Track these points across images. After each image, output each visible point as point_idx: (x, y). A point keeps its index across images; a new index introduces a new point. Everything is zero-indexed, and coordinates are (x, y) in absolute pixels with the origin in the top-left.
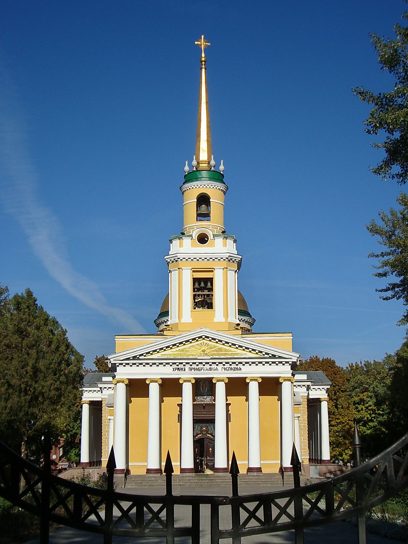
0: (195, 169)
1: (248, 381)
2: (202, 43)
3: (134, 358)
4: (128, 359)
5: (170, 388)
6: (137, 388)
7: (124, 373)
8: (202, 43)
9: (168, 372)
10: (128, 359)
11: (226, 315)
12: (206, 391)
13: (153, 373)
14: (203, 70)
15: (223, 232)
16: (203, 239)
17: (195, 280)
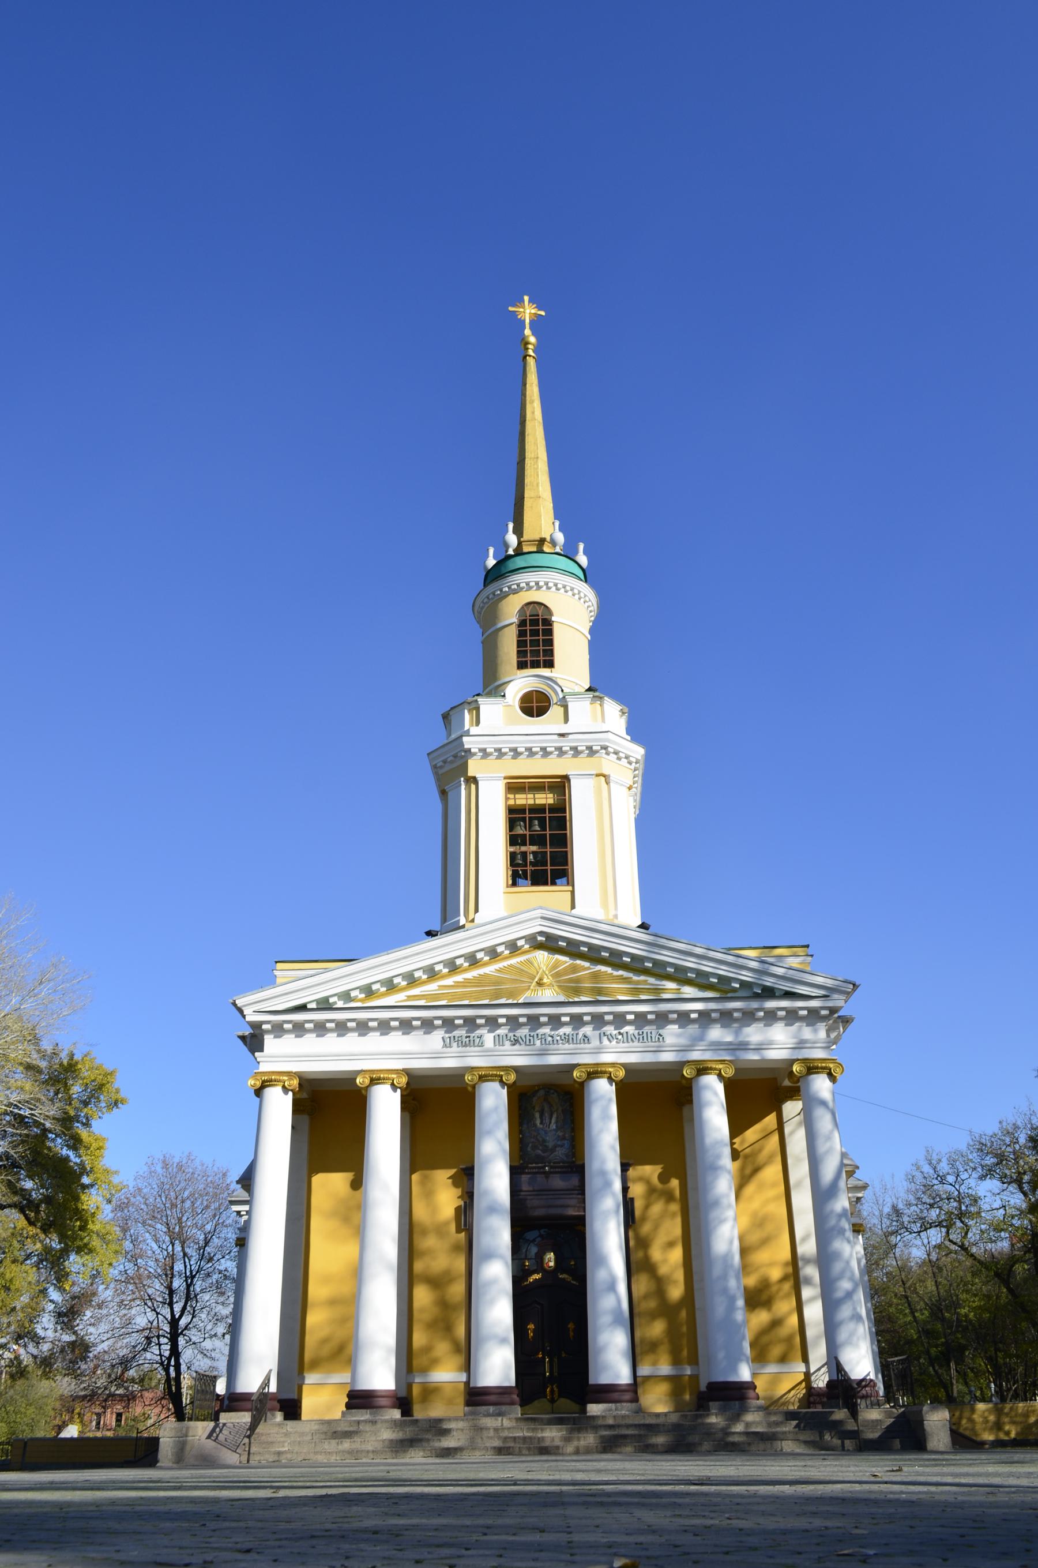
0: (511, 552)
1: (687, 1072)
2: (528, 311)
3: (324, 1005)
4: (302, 1008)
5: (437, 1110)
6: (329, 1114)
7: (289, 1055)
8: (528, 311)
9: (429, 1053)
10: (302, 1008)
11: (609, 892)
12: (553, 1126)
13: (382, 1057)
14: (531, 363)
15: (589, 690)
16: (535, 705)
17: (515, 815)
